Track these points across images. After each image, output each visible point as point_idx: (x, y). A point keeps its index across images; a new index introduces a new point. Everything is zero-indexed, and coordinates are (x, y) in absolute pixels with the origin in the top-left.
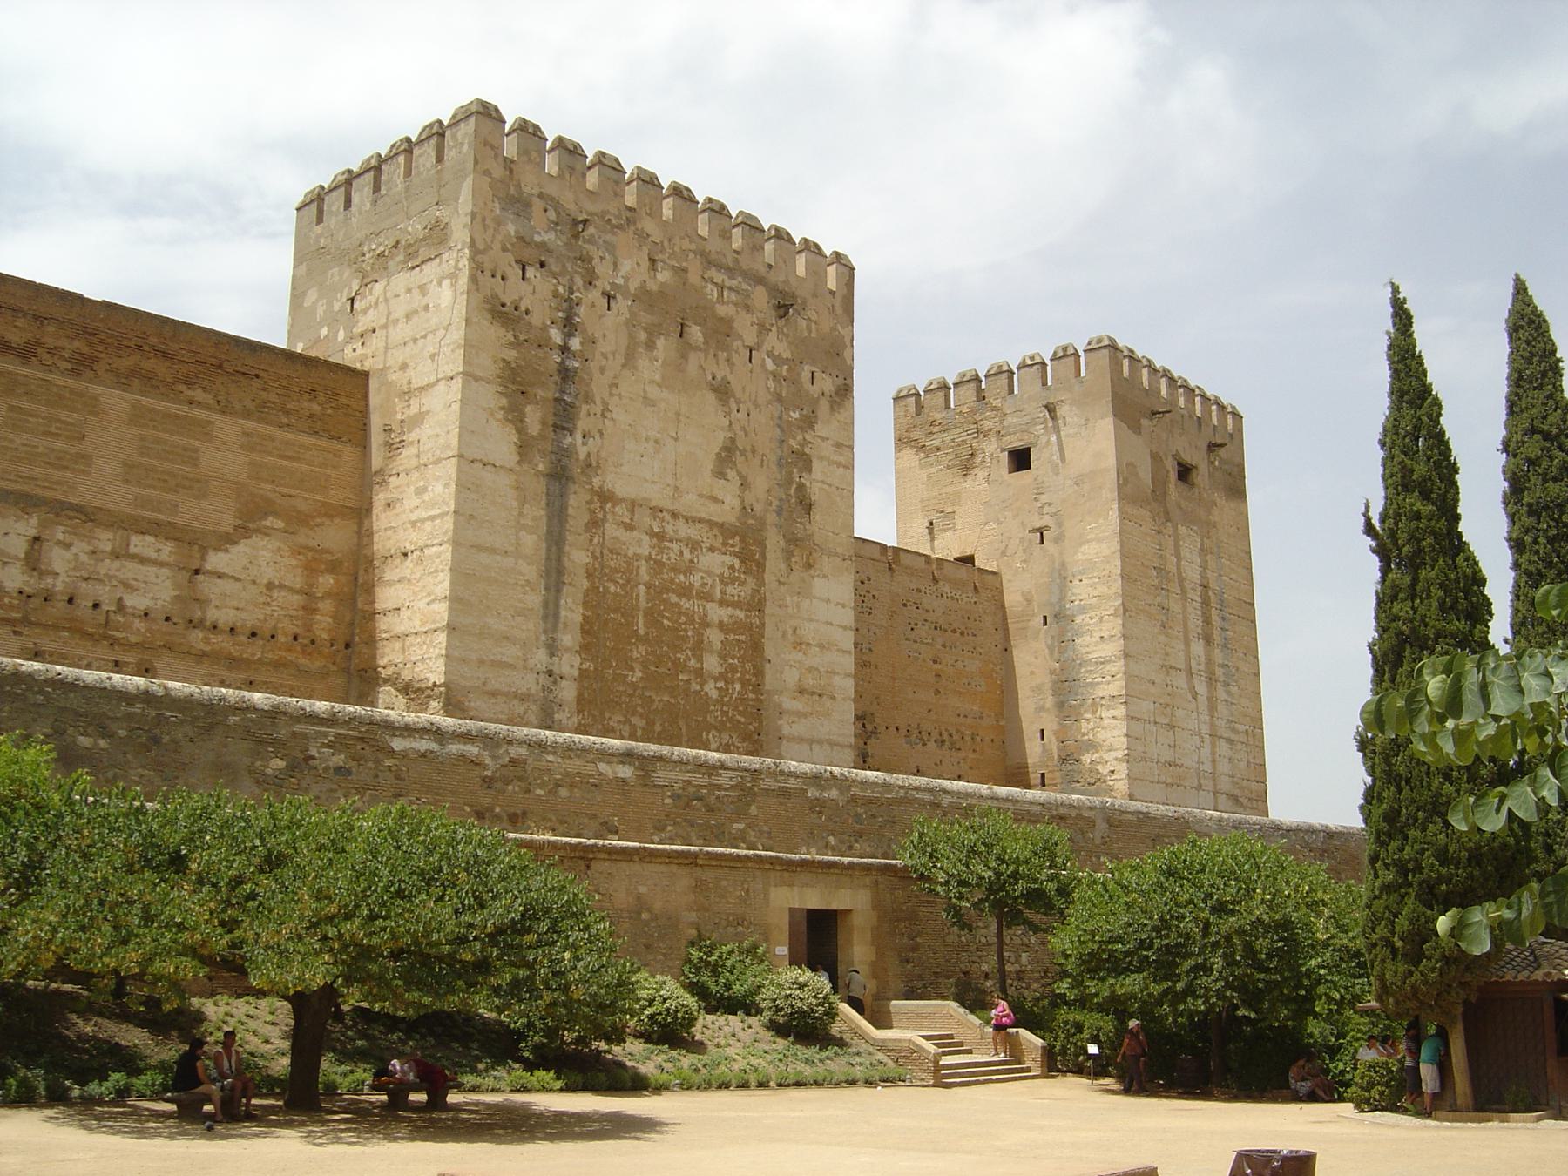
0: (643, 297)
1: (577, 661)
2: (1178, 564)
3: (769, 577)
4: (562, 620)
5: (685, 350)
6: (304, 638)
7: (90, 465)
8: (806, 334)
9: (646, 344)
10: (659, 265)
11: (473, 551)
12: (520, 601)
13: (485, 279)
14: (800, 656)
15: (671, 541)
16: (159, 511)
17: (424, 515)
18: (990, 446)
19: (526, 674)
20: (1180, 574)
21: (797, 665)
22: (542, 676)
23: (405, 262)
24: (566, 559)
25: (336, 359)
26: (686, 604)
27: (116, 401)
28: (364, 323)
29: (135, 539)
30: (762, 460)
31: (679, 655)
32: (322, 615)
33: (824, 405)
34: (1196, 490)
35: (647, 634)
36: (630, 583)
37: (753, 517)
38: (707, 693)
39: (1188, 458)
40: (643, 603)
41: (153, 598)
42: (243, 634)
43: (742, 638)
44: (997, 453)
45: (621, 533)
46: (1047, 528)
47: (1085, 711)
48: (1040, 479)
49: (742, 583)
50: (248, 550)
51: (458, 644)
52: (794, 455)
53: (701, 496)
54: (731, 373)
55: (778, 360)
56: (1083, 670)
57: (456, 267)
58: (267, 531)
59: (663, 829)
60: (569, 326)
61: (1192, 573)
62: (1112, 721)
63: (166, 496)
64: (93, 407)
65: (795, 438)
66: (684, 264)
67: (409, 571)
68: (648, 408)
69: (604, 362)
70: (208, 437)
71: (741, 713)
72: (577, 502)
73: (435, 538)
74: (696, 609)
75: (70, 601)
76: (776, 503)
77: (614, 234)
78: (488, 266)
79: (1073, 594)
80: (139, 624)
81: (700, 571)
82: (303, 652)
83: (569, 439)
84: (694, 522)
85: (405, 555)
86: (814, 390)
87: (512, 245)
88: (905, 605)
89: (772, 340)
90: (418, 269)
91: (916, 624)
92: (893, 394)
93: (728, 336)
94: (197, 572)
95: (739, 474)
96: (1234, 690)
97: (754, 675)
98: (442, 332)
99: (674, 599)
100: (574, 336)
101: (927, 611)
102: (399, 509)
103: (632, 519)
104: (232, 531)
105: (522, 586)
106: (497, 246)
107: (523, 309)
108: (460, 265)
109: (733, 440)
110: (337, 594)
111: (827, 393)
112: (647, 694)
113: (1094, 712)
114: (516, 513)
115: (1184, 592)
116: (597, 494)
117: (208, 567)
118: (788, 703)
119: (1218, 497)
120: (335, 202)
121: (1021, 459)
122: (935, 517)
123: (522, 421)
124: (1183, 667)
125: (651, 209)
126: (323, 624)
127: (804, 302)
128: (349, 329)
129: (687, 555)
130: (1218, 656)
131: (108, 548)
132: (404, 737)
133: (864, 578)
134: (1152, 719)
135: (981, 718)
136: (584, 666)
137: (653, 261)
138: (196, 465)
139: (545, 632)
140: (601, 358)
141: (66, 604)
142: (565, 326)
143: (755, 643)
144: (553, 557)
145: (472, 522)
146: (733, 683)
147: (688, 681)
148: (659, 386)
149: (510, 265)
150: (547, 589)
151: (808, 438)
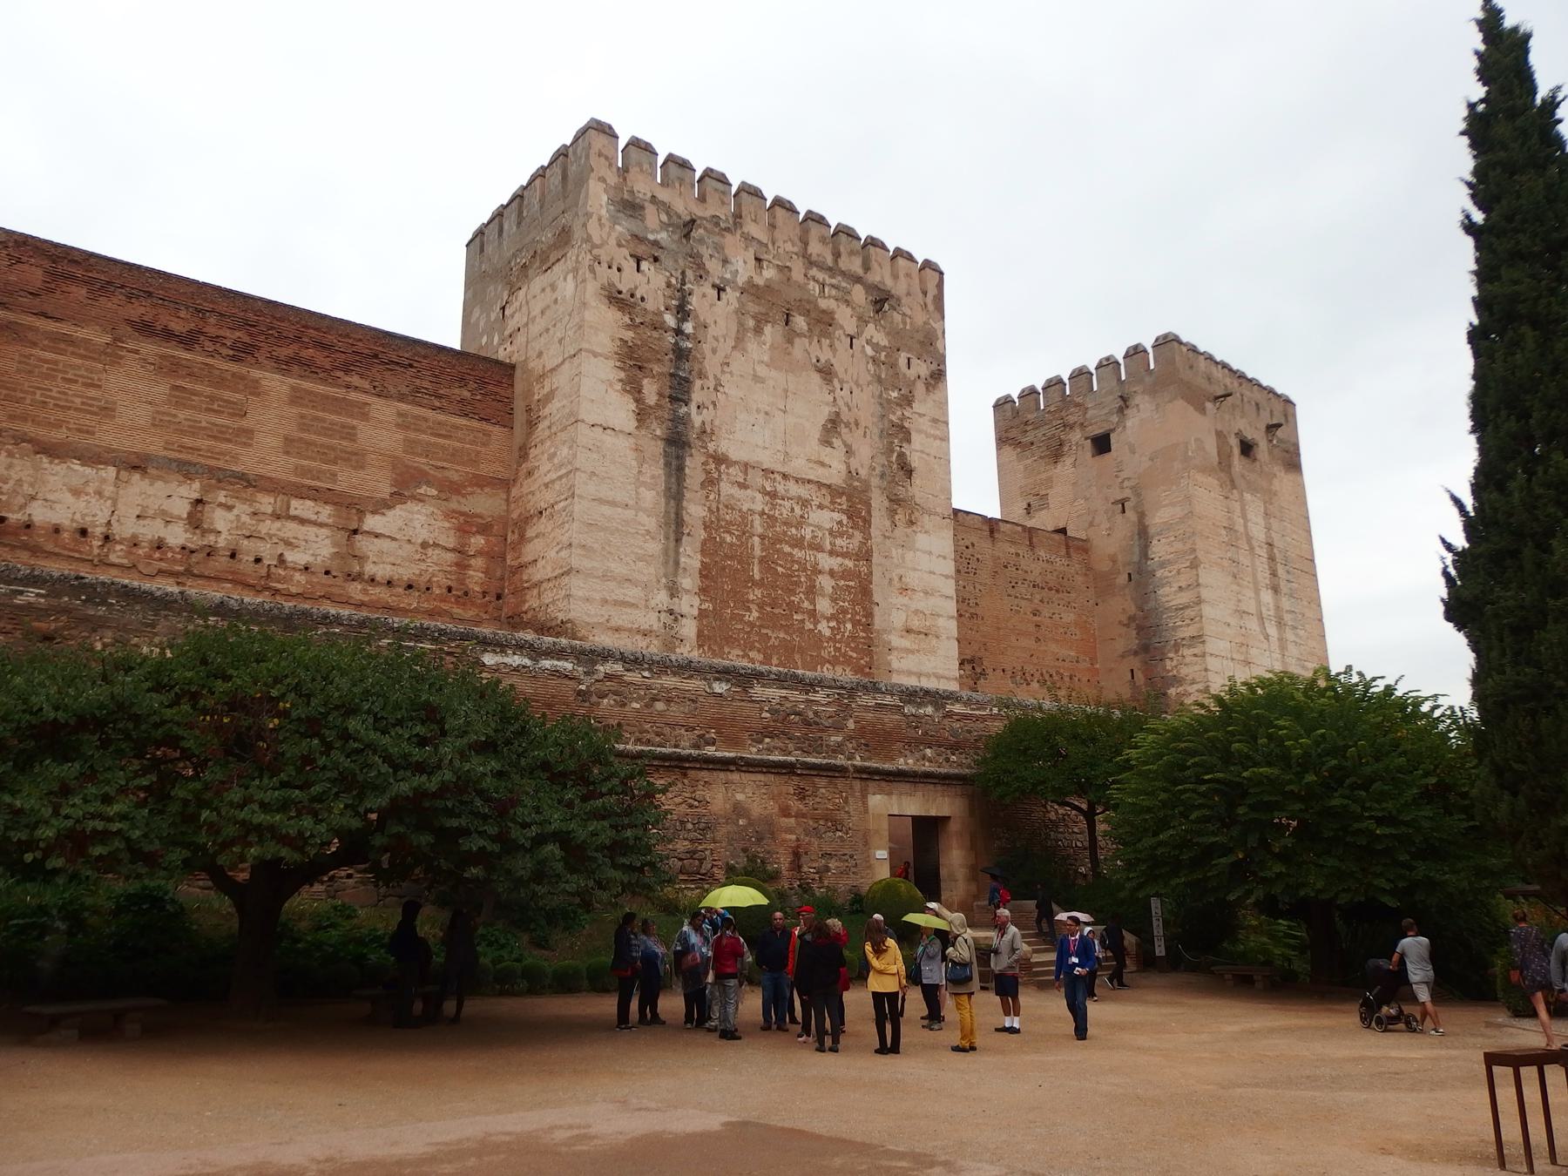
0: (751, 290)
1: (696, 601)
2: (1246, 527)
3: (874, 531)
4: (682, 565)
5: (791, 336)
6: (457, 590)
7: (252, 439)
9: (755, 330)
10: (765, 264)
11: (595, 503)
13: (602, 270)
14: (905, 600)
16: (318, 479)
17: (555, 476)
18: (1076, 436)
20: (1247, 534)
21: (904, 608)
22: (663, 615)
23: (540, 267)
25: (494, 357)
26: (798, 553)
27: (276, 384)
28: (512, 325)
29: (295, 503)
30: (865, 432)
31: (793, 598)
33: (920, 387)
34: (1258, 463)
36: (745, 533)
37: (857, 480)
39: (1249, 435)
40: (758, 552)
41: (313, 555)
42: (400, 586)
43: (852, 583)
44: (1082, 441)
45: (736, 491)
46: (1127, 499)
47: (1169, 651)
48: (1119, 460)
49: (850, 537)
51: (582, 585)
53: (809, 460)
55: (876, 347)
57: (577, 261)
59: (761, 742)
60: (683, 312)
61: (1258, 533)
63: (325, 467)
64: (254, 388)
65: (894, 413)
66: (788, 264)
68: (758, 385)
69: (715, 344)
70: (365, 417)
71: (853, 650)
72: (694, 466)
75: (233, 556)
76: (878, 470)
77: (723, 236)
78: (604, 258)
79: (1154, 553)
80: (298, 576)
81: (812, 525)
82: (457, 602)
83: (685, 409)
86: (912, 374)
88: (1006, 567)
89: (870, 330)
92: (993, 402)
93: (830, 325)
94: (355, 532)
95: (846, 445)
96: (1302, 633)
97: (864, 616)
98: (568, 317)
99: (787, 549)
100: (687, 321)
101: (1026, 572)
102: (536, 475)
103: (745, 479)
106: (612, 242)
107: (638, 296)
108: (580, 259)
109: (838, 414)
110: (487, 553)
111: (923, 376)
113: (1177, 652)
115: (1252, 549)
116: (712, 456)
117: (365, 528)
118: (896, 641)
119: (1278, 470)
120: (492, 233)
121: (1102, 444)
122: (1032, 500)
123: (640, 392)
126: (476, 578)
127: (899, 300)
130: (1286, 603)
131: (269, 510)
132: (495, 652)
133: (968, 543)
136: (703, 607)
137: (758, 260)
138: (354, 441)
139: (665, 576)
140: (713, 340)
141: (228, 559)
142: (678, 313)
143: (864, 588)
144: (673, 510)
145: (594, 478)
146: (844, 623)
147: (803, 621)
149: (626, 259)
150: (667, 538)
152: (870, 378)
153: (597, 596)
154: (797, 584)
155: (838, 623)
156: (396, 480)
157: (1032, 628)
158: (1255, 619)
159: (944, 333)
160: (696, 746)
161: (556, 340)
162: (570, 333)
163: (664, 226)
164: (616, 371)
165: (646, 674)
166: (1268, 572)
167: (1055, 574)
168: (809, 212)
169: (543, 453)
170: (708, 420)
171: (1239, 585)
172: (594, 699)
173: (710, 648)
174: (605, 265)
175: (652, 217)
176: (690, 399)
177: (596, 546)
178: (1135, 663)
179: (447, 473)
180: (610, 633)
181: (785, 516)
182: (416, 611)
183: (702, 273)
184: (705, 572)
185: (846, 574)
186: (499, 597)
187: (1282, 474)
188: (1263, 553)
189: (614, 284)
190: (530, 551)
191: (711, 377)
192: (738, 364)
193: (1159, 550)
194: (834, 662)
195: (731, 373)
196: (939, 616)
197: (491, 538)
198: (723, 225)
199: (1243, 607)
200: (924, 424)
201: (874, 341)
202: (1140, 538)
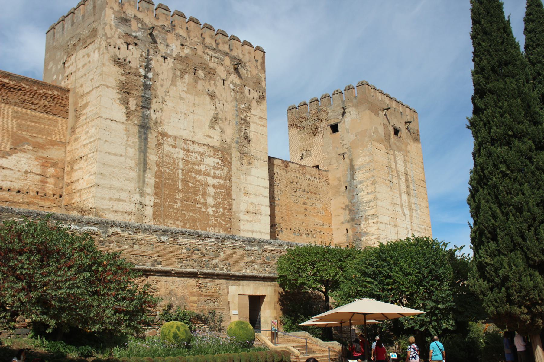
0: (179, 58)
1: (152, 199)
2: (396, 166)
3: (233, 167)
4: (146, 182)
5: (197, 79)
6: (41, 193)
8: (246, 76)
11: (107, 154)
12: (127, 174)
13: (111, 49)
15: (192, 153)
17: (87, 141)
19: (130, 204)
22: (137, 205)
23: (82, 46)
24: (147, 158)
26: (199, 177)
28: (68, 71)
30: (229, 123)
31: (196, 197)
32: (49, 184)
33: (254, 103)
34: (401, 139)
35: (183, 189)
36: (175, 167)
37: (226, 144)
38: (208, 212)
39: (398, 126)
40: (180, 176)
42: (14, 191)
43: (223, 191)
44: (326, 127)
47: (363, 221)
49: (222, 170)
50: (17, 158)
52: (243, 121)
53: (204, 135)
54: (216, 89)
55: (235, 85)
56: (361, 205)
57: (100, 44)
58: (25, 151)
59: (182, 263)
60: (148, 68)
61: (401, 169)
62: (373, 224)
65: (242, 114)
66: (195, 47)
67: (82, 164)
71: (223, 220)
72: (152, 137)
73: (92, 150)
74: (203, 179)
76: (235, 139)
78: (112, 43)
82: (41, 199)
83: (148, 112)
84: (201, 145)
85: (81, 158)
86: (251, 97)
87: (123, 36)
88: (292, 183)
90: (86, 48)
91: (297, 190)
92: (287, 109)
93: (214, 75)
95: (221, 129)
97: (228, 205)
99: (194, 175)
100: (150, 72)
101: (301, 185)
102: (79, 141)
103: (175, 144)
104: (9, 150)
105: (128, 169)
106: (116, 36)
108: (101, 43)
109: (217, 114)
110: (56, 176)
111: (255, 98)
112: (183, 212)
113: (366, 221)
114: (125, 140)
115: (398, 176)
118: (242, 216)
119: (410, 141)
121: (335, 128)
122: (304, 152)
124: (399, 204)
125: (181, 25)
127: (245, 64)
128: (63, 74)
129: (199, 158)
130: (413, 200)
134: (388, 223)
135: (323, 225)
136: (156, 201)
137: (182, 45)
139: (139, 187)
142: (146, 68)
144: (142, 158)
145: (107, 143)
146: (219, 208)
147: (201, 208)
148: (186, 93)
149: (122, 44)
150: (140, 170)
151: (248, 115)
152: (232, 99)
153: (107, 197)
154: (199, 191)
155: (217, 208)
156: (13, 142)
157: (303, 210)
158: (400, 206)
159: (265, 79)
160: (153, 265)
161: (89, 79)
162: (96, 77)
163: (140, 29)
164: (117, 94)
165: (131, 232)
166: (405, 186)
167: (314, 186)
168: (206, 24)
169: (82, 131)
170: (159, 117)
171: (393, 192)
172: (107, 244)
173: (158, 219)
174: (112, 47)
175: (135, 25)
176: (151, 107)
177: (107, 174)
178: (348, 226)
179: (37, 140)
180: (113, 213)
181: (193, 160)
182: (22, 203)
183: (157, 51)
184: (157, 186)
185: (220, 187)
186: (61, 196)
187: (412, 143)
188: (403, 177)
189: (116, 55)
190: (76, 176)
191: (160, 98)
192: (173, 92)
193: (359, 176)
194: (215, 226)
195: (169, 96)
196: (262, 205)
197: (57, 169)
198: (167, 29)
199: (395, 201)
200: (256, 119)
201: (234, 82)
202: (350, 171)
